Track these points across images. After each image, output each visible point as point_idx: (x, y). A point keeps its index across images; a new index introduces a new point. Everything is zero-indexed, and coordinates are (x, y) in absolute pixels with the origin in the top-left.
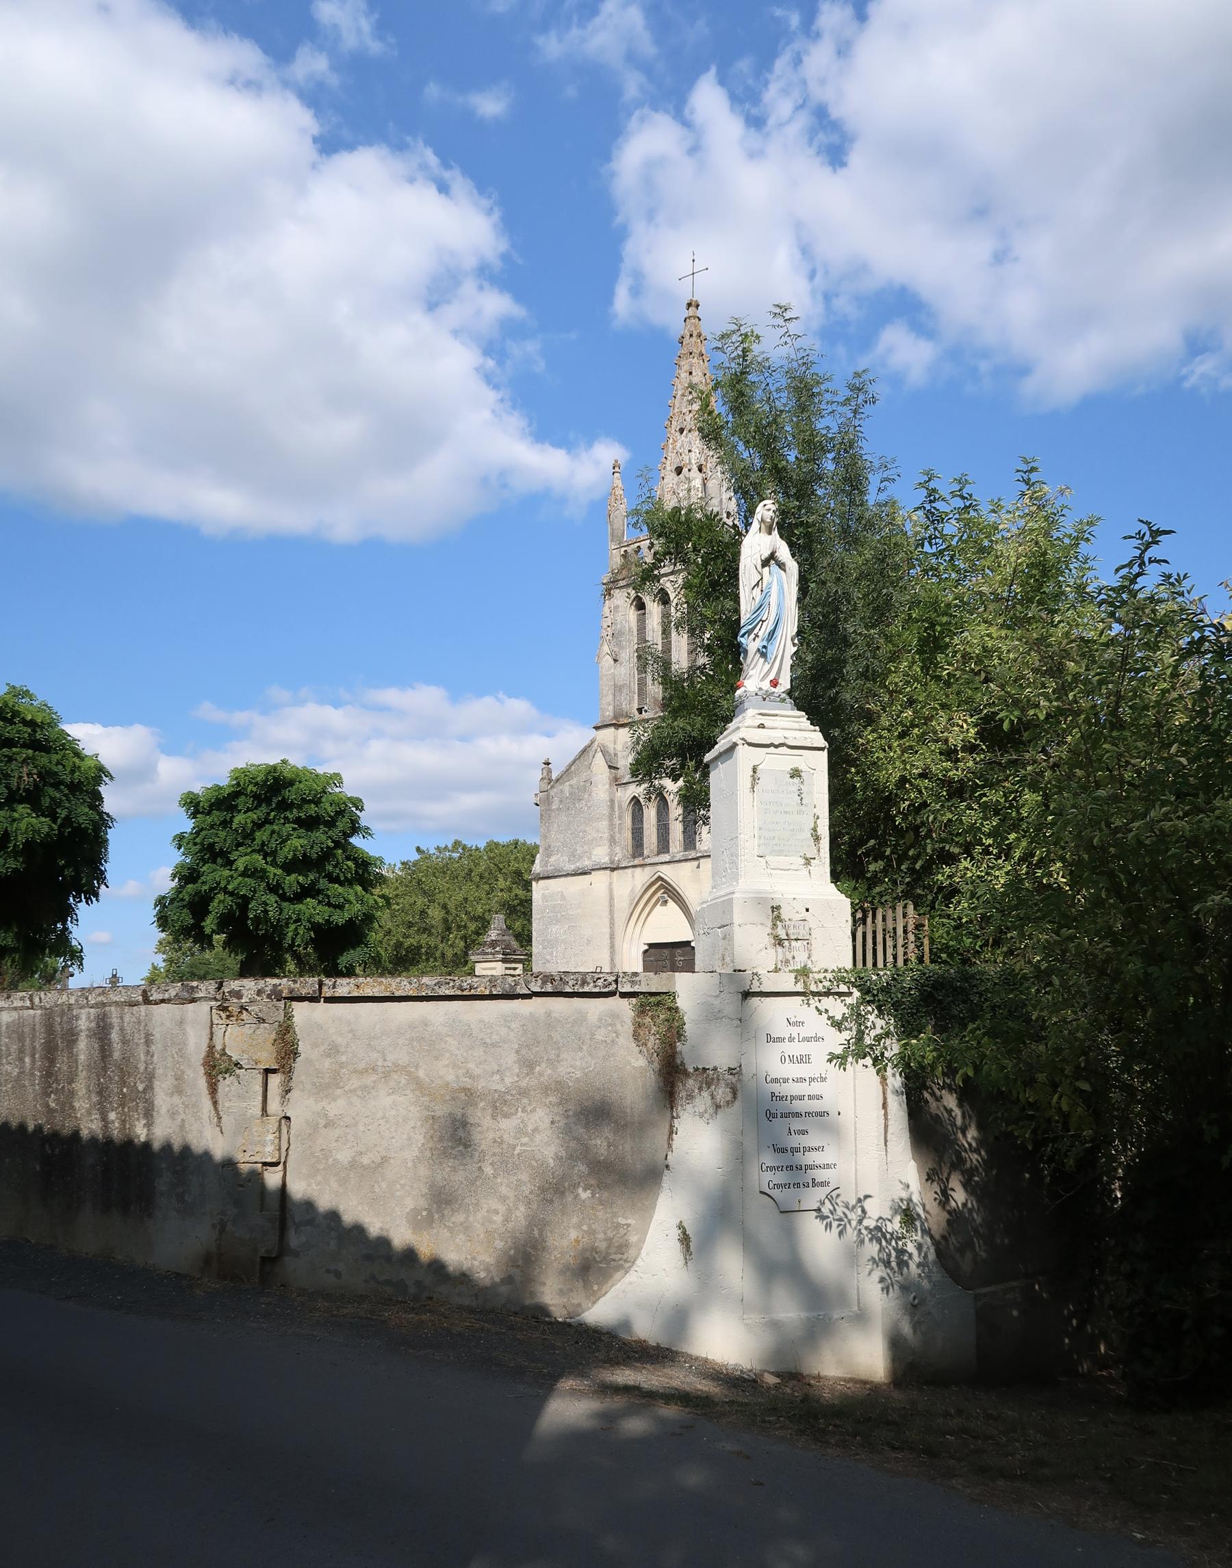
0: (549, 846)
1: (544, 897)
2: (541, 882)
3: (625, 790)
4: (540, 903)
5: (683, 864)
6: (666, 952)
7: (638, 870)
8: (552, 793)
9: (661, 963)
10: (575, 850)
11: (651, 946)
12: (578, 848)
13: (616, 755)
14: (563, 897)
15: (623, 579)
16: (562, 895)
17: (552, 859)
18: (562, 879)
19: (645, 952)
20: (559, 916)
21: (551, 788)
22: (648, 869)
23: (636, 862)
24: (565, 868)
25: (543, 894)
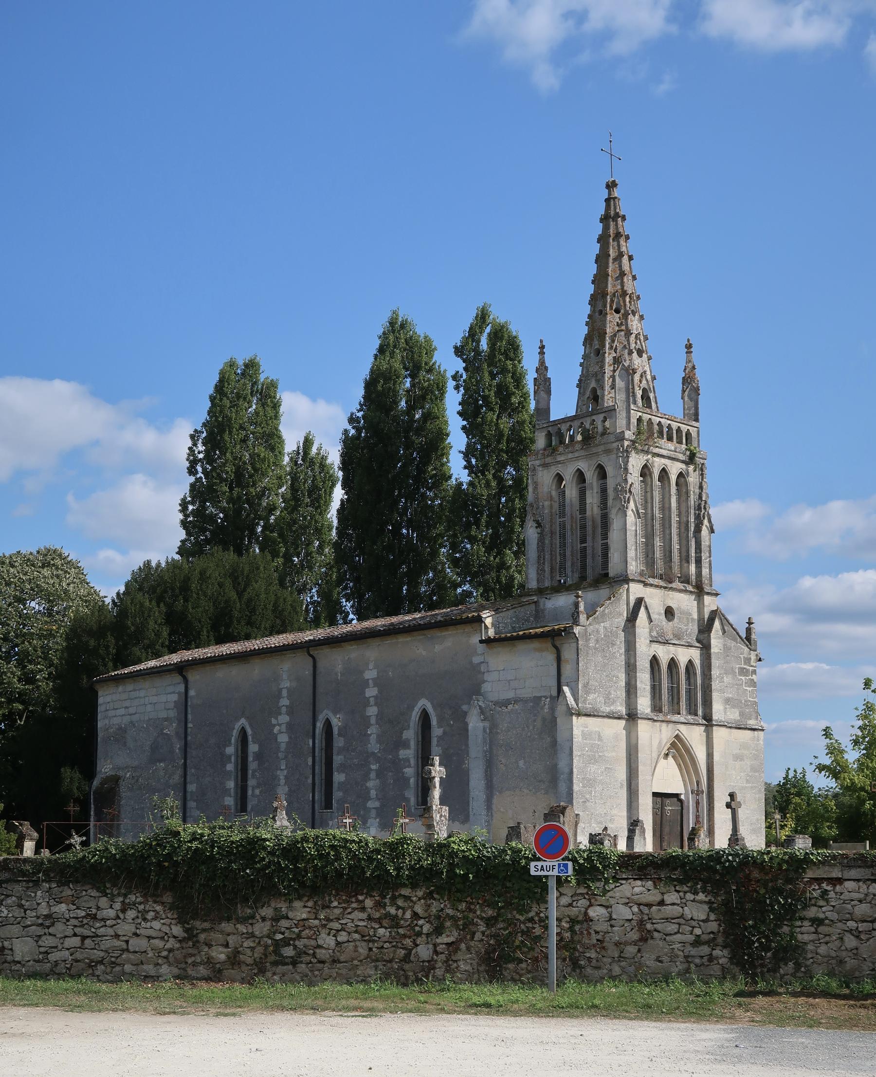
0: (588, 683)
1: (584, 735)
2: (583, 720)
5: (695, 727)
7: (664, 725)
10: (610, 693)
12: (612, 692)
14: (600, 738)
16: (599, 736)
17: (591, 697)
18: (599, 720)
20: (597, 756)
22: (671, 725)
23: (661, 717)
25: (583, 731)
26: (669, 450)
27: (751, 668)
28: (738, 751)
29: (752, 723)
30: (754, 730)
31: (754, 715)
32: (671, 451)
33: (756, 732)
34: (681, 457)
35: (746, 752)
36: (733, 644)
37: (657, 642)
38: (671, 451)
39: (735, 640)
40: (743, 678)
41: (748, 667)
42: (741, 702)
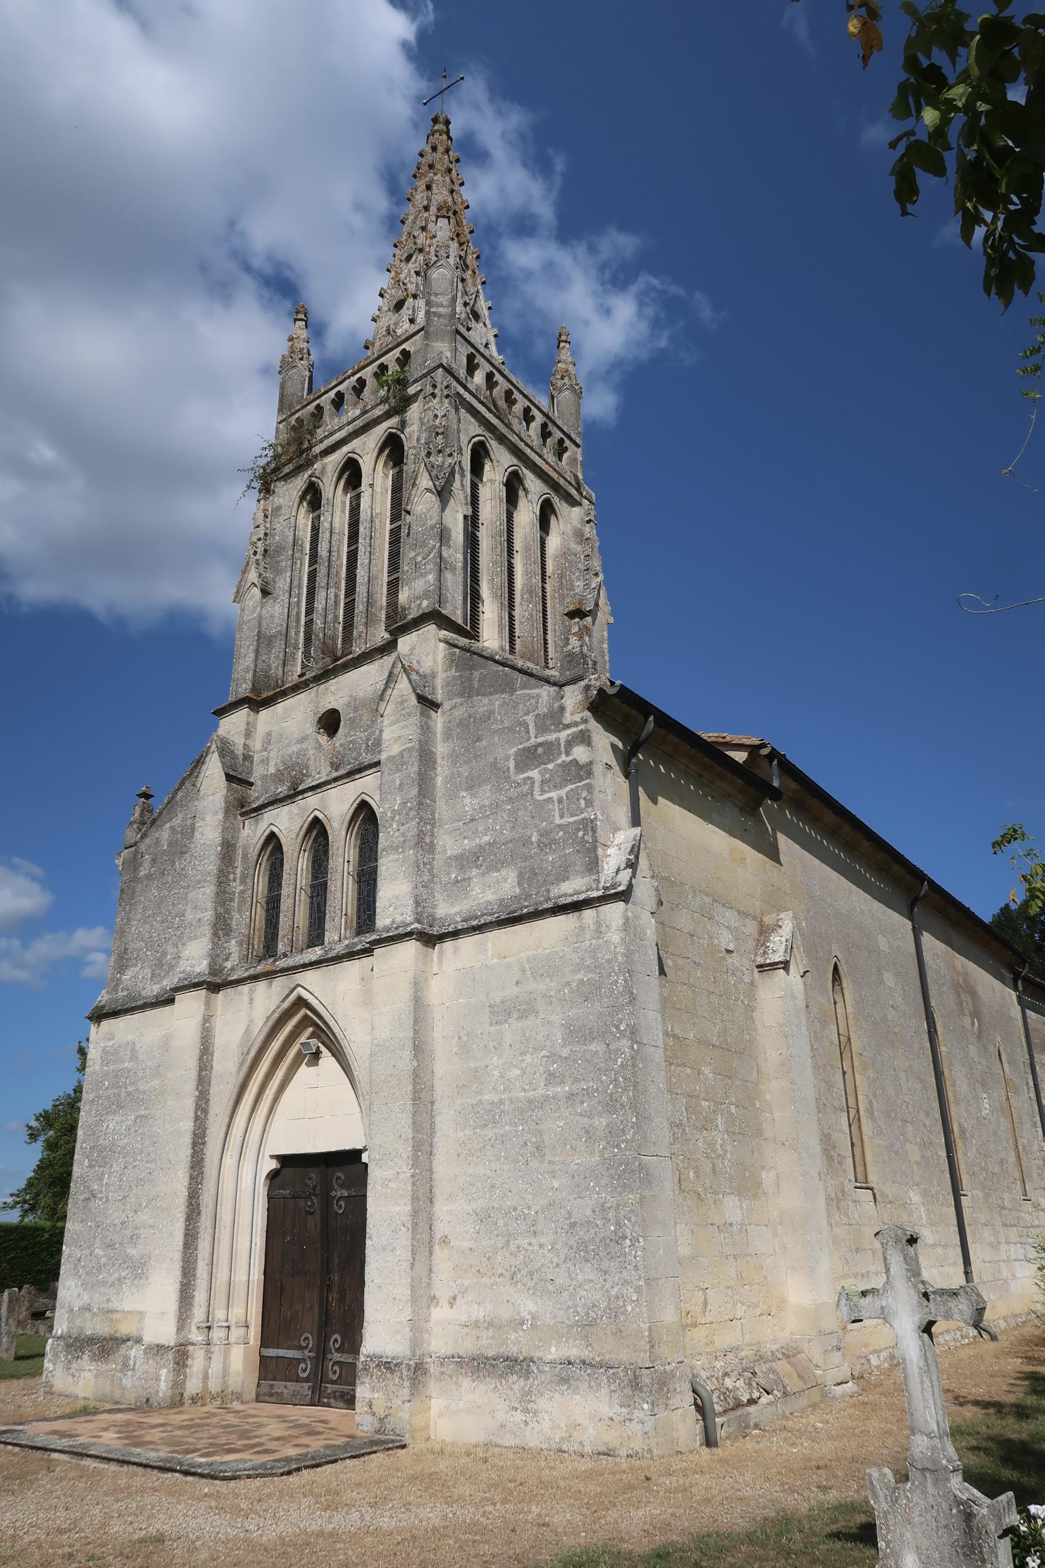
3: (257, 822)
4: (97, 1068)
6: (314, 1175)
7: (261, 986)
8: (142, 847)
9: (301, 1202)
11: (285, 1160)
13: (247, 757)
15: (290, 461)
19: (273, 1176)
21: (142, 838)
24: (144, 993)
26: (349, 423)
27: (564, 735)
28: (512, 991)
29: (572, 887)
30: (576, 907)
31: (580, 862)
32: (354, 420)
33: (588, 914)
34: (378, 412)
35: (541, 986)
36: (497, 701)
37: (272, 803)
38: (354, 420)
39: (509, 687)
40: (535, 774)
41: (551, 737)
42: (526, 842)
